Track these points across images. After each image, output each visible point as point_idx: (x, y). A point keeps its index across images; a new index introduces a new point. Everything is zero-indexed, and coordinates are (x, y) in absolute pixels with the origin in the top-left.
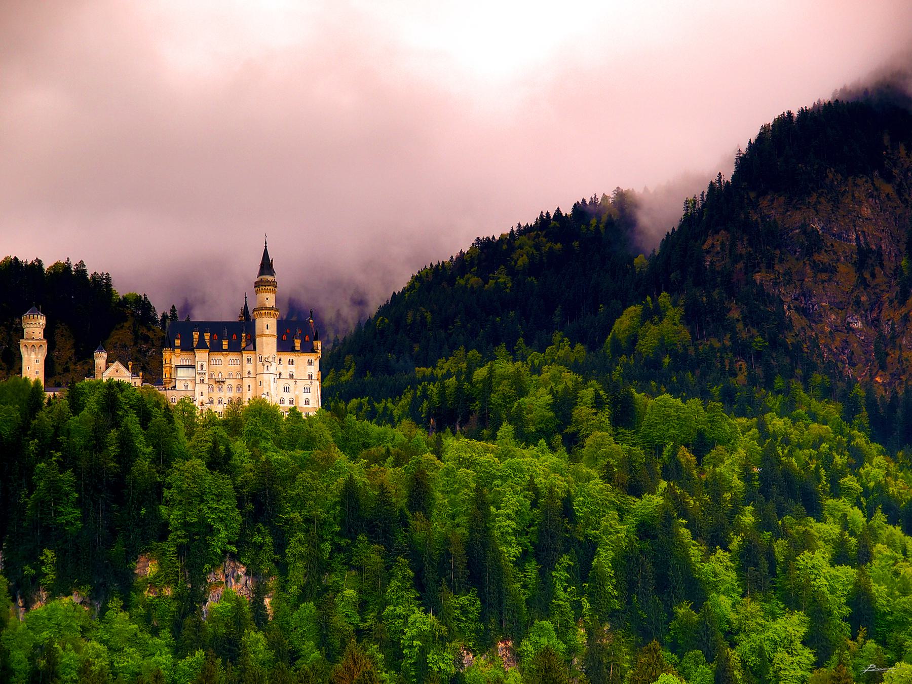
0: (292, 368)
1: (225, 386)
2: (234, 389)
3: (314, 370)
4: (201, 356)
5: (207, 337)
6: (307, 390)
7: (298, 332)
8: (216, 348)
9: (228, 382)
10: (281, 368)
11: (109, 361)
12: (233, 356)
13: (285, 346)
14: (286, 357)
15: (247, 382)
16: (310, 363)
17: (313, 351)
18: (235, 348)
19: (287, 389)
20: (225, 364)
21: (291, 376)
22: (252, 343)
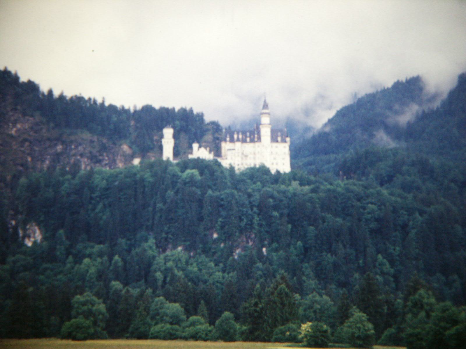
4: (238, 145)
5: (240, 136)
6: (283, 159)
7: (279, 134)
8: (244, 141)
11: (200, 147)
12: (252, 145)
13: (274, 139)
14: (275, 144)
16: (285, 147)
17: (285, 142)
18: (252, 141)
19: (275, 159)
20: (249, 147)
22: (259, 139)
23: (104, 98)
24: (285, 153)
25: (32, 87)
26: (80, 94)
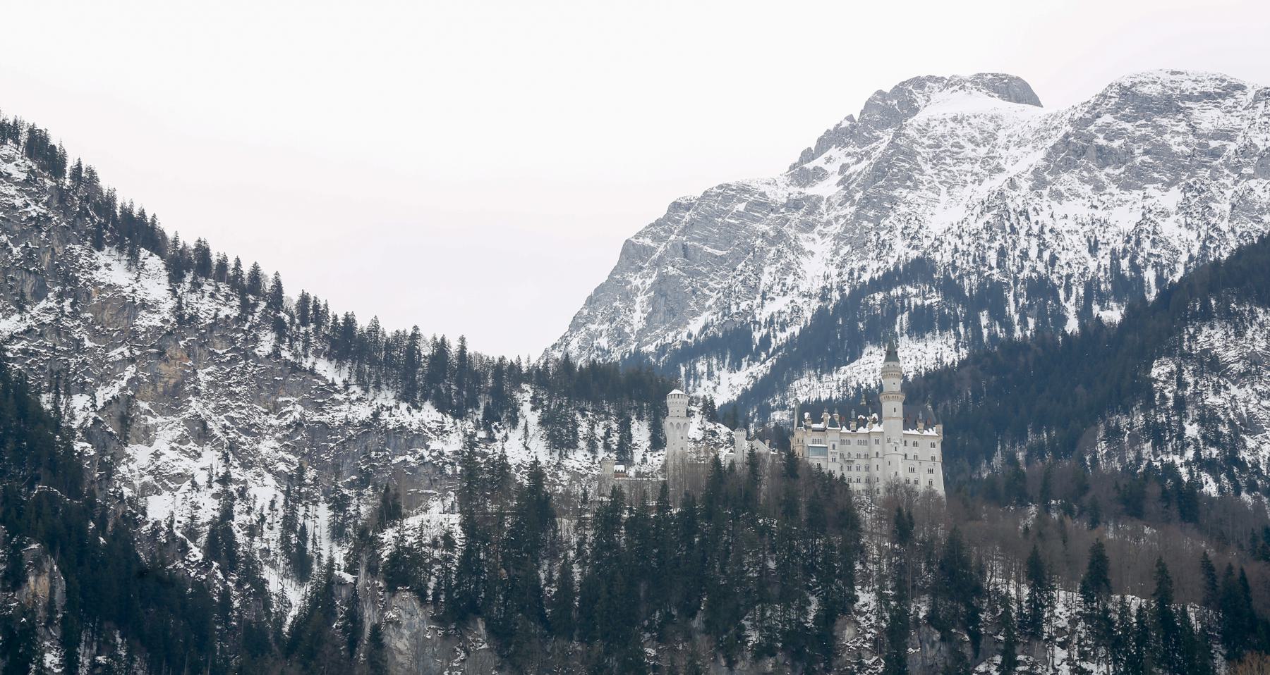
0: (916, 450)
1: (854, 467)
2: (863, 469)
6: (930, 471)
9: (857, 462)
10: (906, 450)
15: (875, 462)
19: (912, 470)
21: (916, 457)
23: (462, 339)
24: (933, 458)
26: (416, 328)
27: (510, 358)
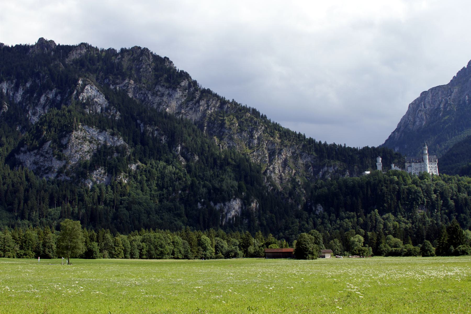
3: (436, 165)
4: (413, 164)
11: (394, 166)
12: (419, 163)
13: (430, 161)
14: (430, 163)
15: (422, 169)
18: (420, 162)
25: (311, 141)
27: (356, 147)
